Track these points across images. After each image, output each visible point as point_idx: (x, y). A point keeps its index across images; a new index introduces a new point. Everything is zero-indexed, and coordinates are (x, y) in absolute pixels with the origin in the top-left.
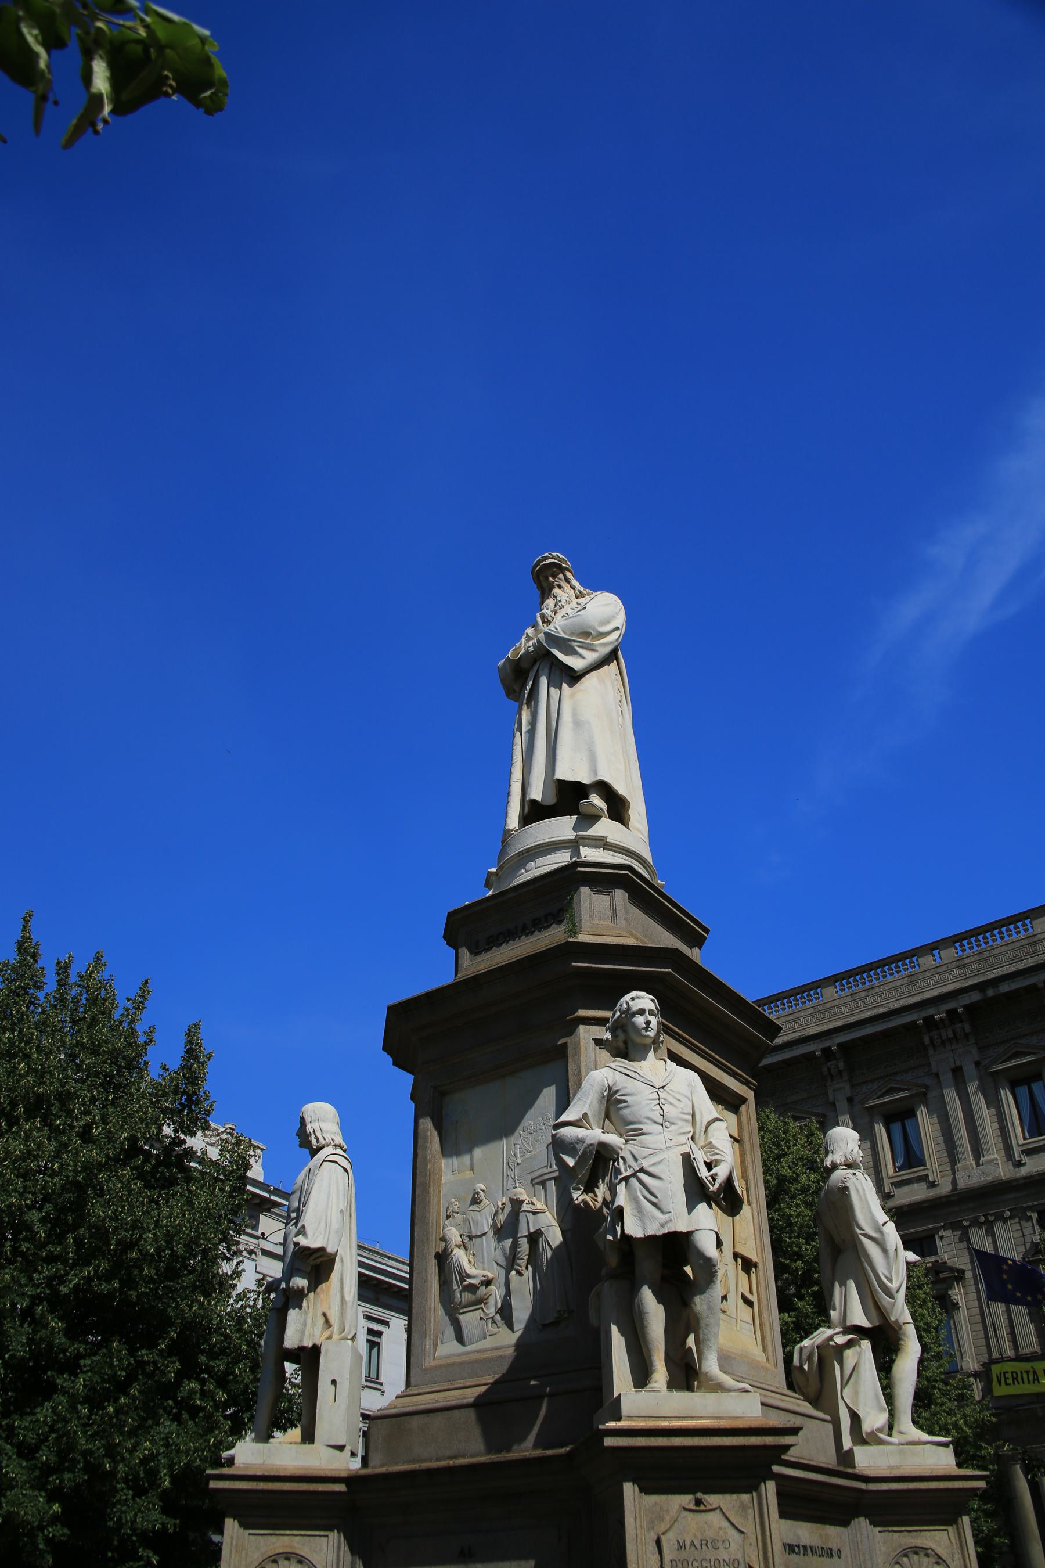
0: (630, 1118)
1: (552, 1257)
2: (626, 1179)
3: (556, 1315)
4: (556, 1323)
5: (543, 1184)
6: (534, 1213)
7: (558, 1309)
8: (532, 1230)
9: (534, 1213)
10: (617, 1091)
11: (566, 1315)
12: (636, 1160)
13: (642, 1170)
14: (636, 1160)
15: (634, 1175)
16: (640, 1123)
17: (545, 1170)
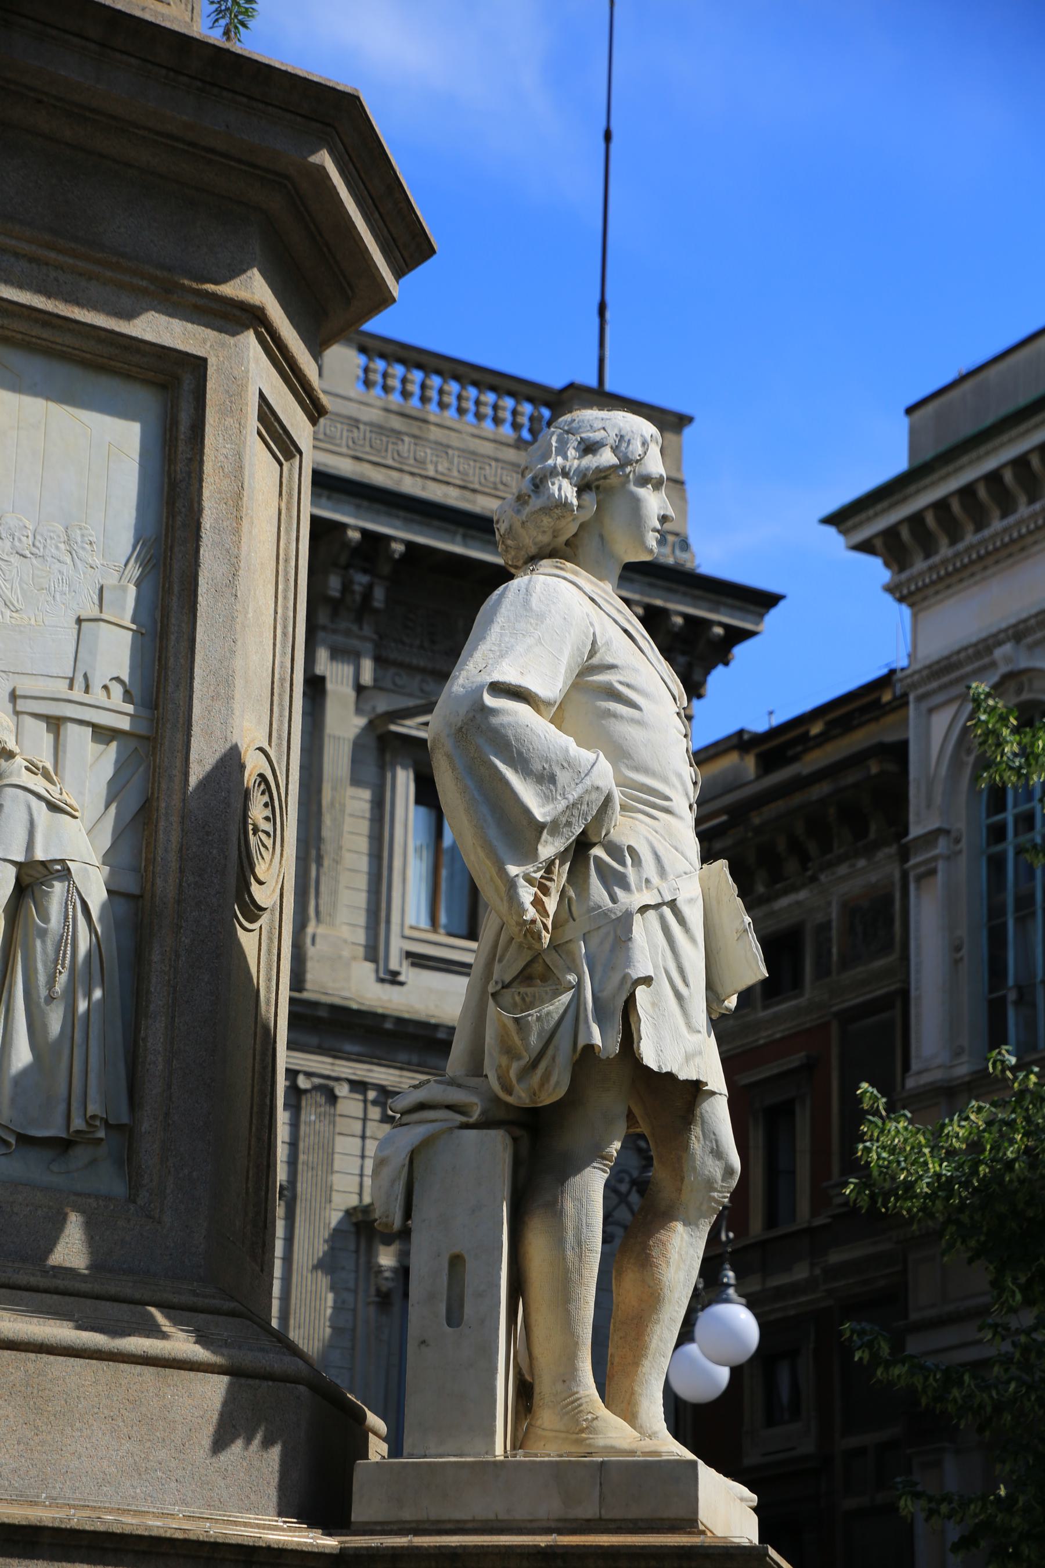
0: (644, 754)
1: (89, 954)
2: (644, 909)
3: (78, 1123)
4: (63, 1145)
5: (55, 724)
6: (53, 807)
7: (93, 1109)
8: (40, 855)
9: (53, 807)
10: (612, 667)
11: (101, 1134)
12: (662, 872)
13: (672, 904)
14: (662, 872)
15: (657, 907)
16: (665, 780)
17: (60, 688)
